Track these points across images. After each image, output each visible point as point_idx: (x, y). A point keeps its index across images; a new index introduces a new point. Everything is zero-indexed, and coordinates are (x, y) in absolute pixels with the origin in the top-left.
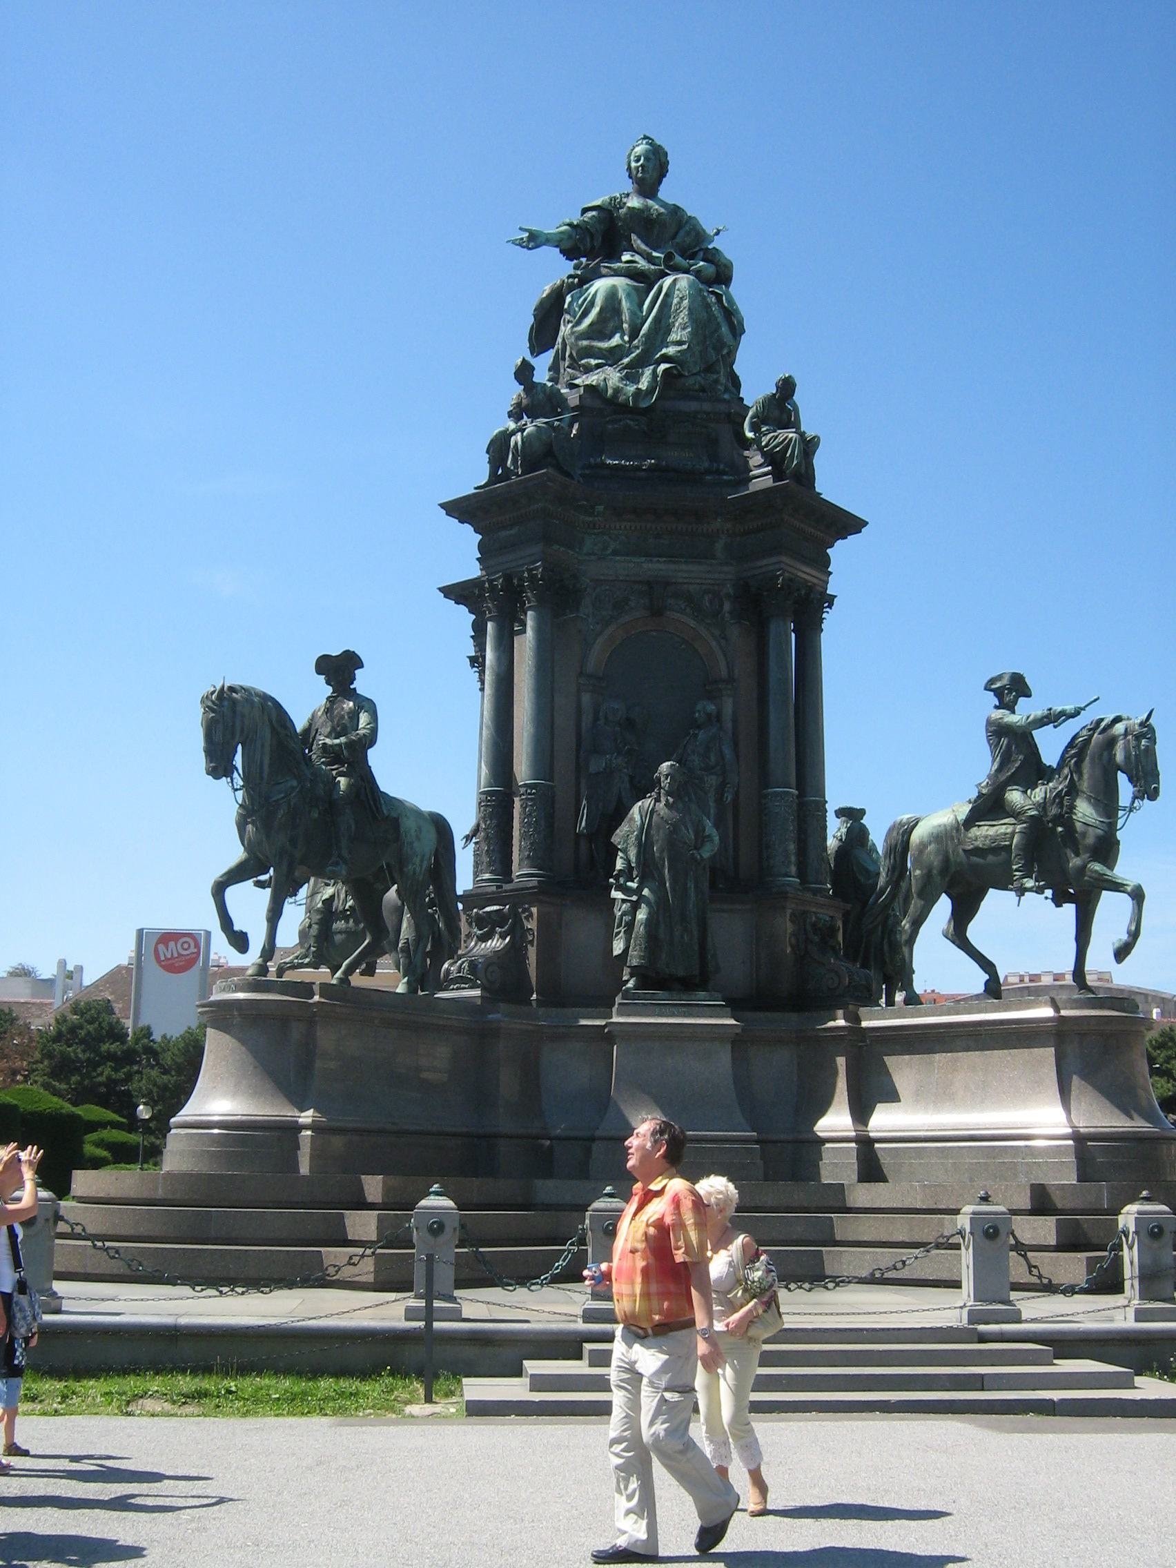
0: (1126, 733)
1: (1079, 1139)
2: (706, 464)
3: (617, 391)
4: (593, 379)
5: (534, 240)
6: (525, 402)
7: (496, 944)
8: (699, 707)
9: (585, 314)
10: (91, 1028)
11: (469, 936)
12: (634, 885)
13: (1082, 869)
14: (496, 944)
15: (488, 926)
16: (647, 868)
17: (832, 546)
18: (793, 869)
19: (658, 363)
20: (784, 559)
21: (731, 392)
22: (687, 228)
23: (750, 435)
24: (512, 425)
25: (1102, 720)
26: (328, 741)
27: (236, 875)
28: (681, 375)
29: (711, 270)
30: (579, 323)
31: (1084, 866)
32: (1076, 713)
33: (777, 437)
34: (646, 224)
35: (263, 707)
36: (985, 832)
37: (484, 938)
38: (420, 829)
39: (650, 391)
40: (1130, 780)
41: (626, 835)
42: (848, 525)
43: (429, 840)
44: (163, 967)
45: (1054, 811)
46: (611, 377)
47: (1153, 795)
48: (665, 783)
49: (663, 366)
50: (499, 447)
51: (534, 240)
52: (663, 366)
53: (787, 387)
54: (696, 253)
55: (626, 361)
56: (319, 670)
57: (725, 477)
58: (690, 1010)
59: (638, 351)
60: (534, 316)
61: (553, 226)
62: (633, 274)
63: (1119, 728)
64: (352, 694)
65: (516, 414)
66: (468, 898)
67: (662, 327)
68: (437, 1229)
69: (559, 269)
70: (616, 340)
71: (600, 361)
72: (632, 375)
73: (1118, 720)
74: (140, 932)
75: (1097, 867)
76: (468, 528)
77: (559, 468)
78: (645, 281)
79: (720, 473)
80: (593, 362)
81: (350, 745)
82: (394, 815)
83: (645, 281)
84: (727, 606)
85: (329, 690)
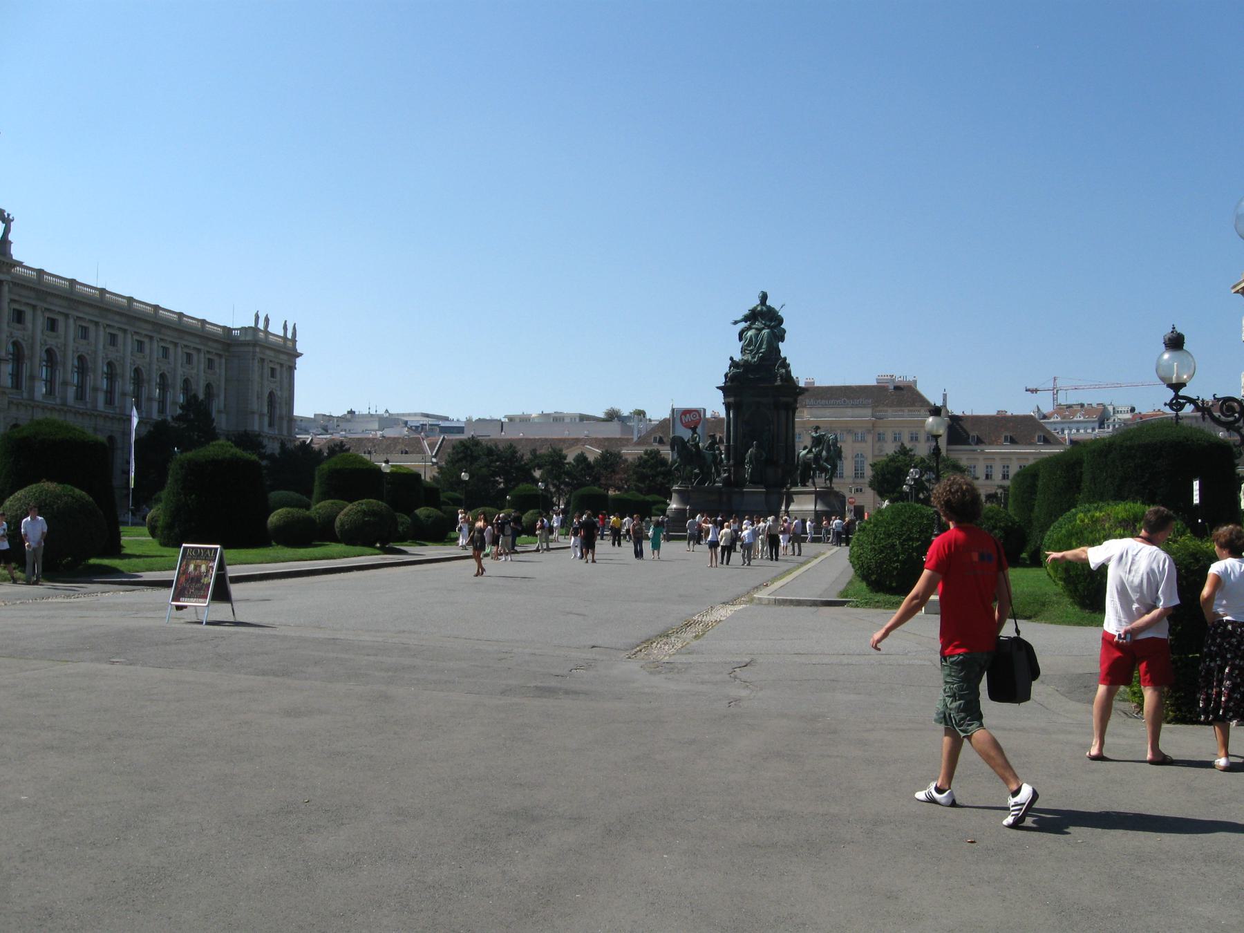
1: (816, 511)
5: (736, 323)
7: (726, 475)
10: (652, 461)
14: (726, 475)
15: (725, 471)
16: (751, 462)
34: (761, 313)
36: (809, 456)
44: (685, 426)
50: (726, 376)
51: (736, 323)
52: (761, 355)
58: (758, 488)
61: (740, 317)
64: (696, 433)
65: (730, 368)
67: (760, 346)
70: (751, 348)
72: (753, 358)
74: (673, 410)
75: (825, 464)
78: (759, 330)
80: (748, 352)
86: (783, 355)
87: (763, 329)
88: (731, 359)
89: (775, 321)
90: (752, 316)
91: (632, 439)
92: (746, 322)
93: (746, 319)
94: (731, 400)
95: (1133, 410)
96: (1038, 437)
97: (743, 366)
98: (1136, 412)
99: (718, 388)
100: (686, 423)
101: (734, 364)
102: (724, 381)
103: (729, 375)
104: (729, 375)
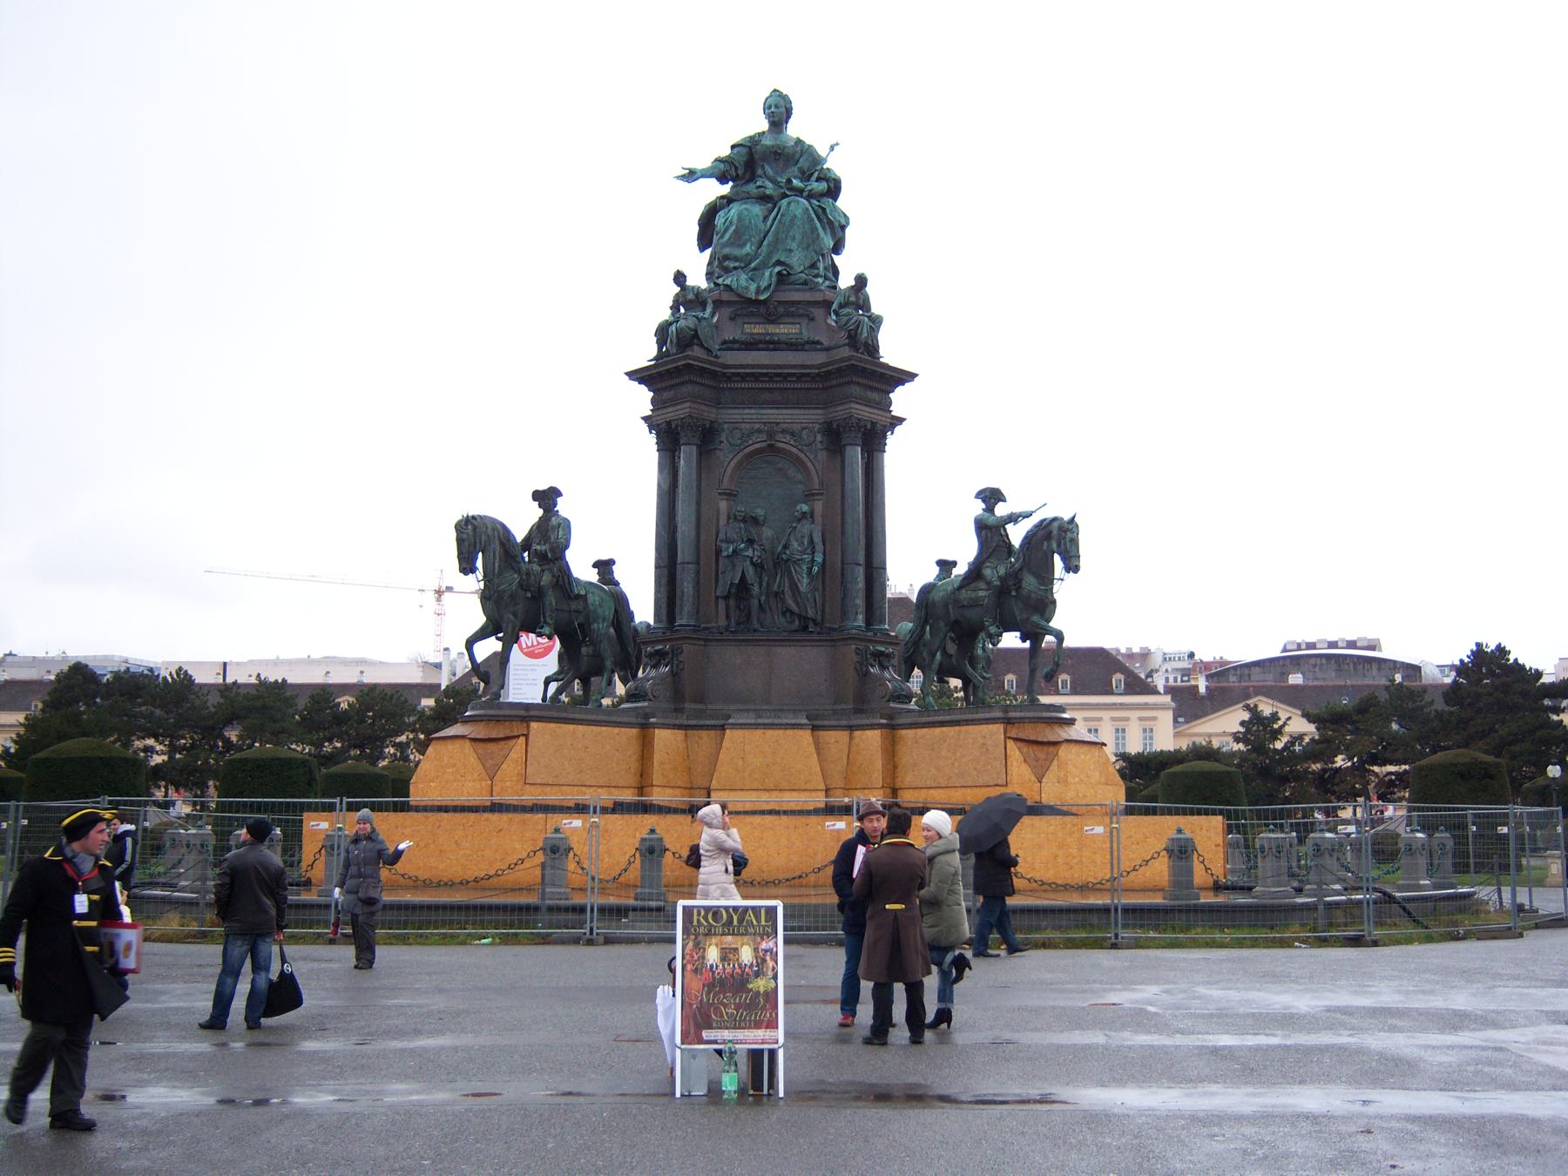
2: (806, 338)
5: (691, 176)
6: (681, 300)
8: (798, 508)
9: (726, 230)
15: (658, 658)
17: (893, 391)
18: (860, 617)
19: (774, 265)
20: (853, 405)
21: (830, 280)
25: (1045, 520)
26: (538, 547)
27: (481, 635)
28: (789, 274)
29: (822, 186)
30: (722, 237)
31: (1028, 619)
32: (1028, 515)
33: (851, 319)
35: (494, 529)
40: (1064, 559)
47: (1076, 569)
49: (778, 269)
50: (662, 332)
51: (691, 176)
52: (778, 269)
53: (861, 281)
54: (813, 174)
55: (753, 265)
56: (534, 499)
57: (819, 347)
60: (699, 225)
61: (704, 162)
62: (764, 199)
63: (1056, 524)
65: (675, 308)
70: (748, 249)
71: (737, 264)
75: (1035, 618)
76: (643, 388)
77: (702, 346)
80: (732, 264)
82: (583, 593)
84: (819, 437)
85: (540, 512)
87: (784, 196)
88: (679, 278)
89: (818, 180)
91: (439, 685)
92: (722, 179)
93: (724, 171)
94: (676, 412)
95: (1191, 655)
98: (1196, 658)
100: (528, 647)
101: (687, 299)
103: (673, 328)
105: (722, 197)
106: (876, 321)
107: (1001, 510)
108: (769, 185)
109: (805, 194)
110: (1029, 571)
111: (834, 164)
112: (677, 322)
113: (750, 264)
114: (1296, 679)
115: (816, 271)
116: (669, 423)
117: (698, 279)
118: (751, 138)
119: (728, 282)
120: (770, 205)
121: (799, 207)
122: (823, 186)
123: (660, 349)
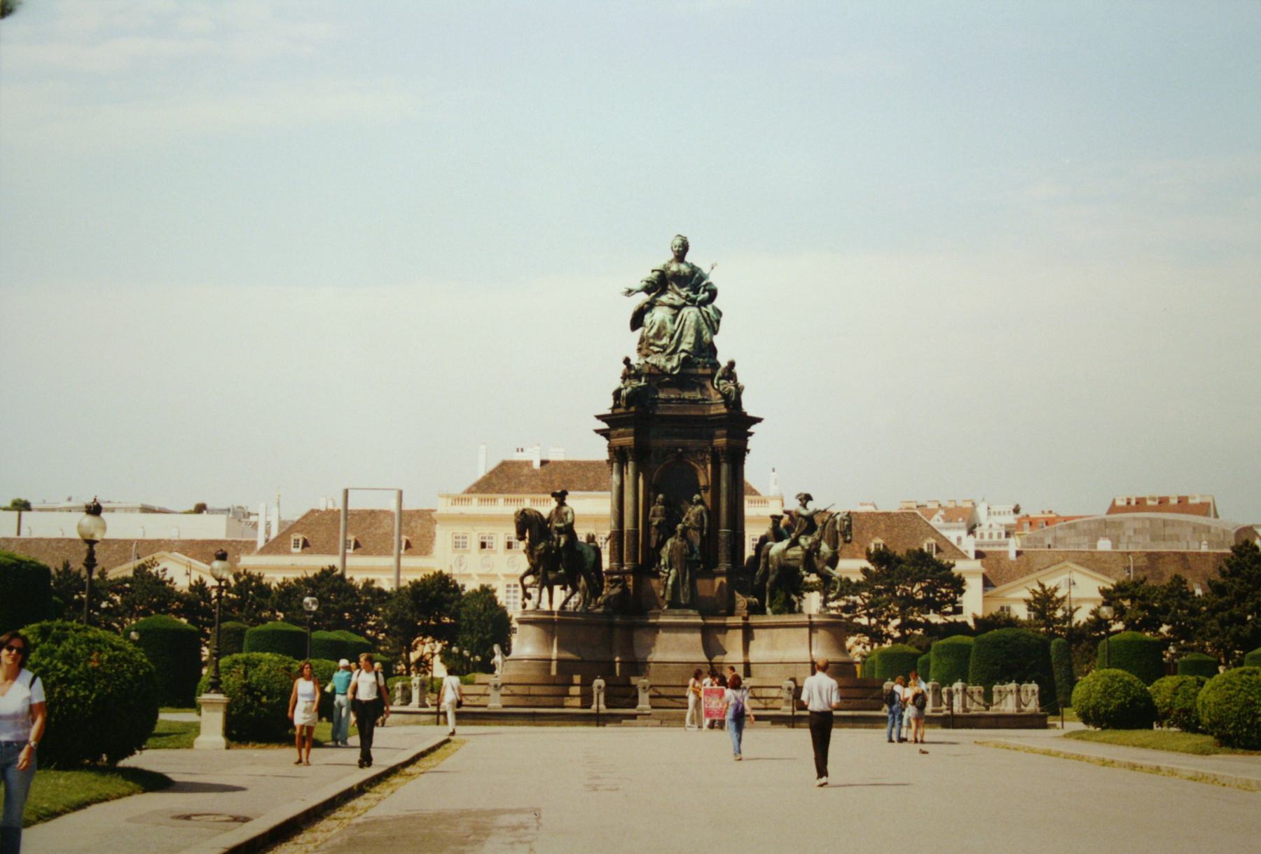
0: (841, 519)
3: (665, 367)
4: (653, 360)
9: (652, 328)
11: (608, 586)
12: (667, 571)
13: (823, 568)
14: (617, 590)
22: (697, 275)
23: (716, 387)
24: (622, 386)
30: (649, 331)
37: (613, 587)
38: (589, 554)
39: (677, 367)
41: (665, 553)
42: (757, 420)
43: (593, 555)
45: (813, 547)
46: (659, 360)
48: (679, 533)
50: (617, 394)
52: (683, 355)
53: (732, 365)
59: (672, 348)
62: (672, 306)
66: (609, 573)
68: (599, 687)
69: (643, 298)
70: (665, 341)
73: (838, 514)
75: (828, 568)
78: (677, 309)
79: (706, 400)
80: (656, 349)
81: (566, 526)
83: (677, 309)
86: (723, 359)
87: (684, 305)
88: (627, 361)
90: (659, 284)
91: (254, 543)
92: (647, 290)
96: (928, 545)
97: (649, 375)
98: (1023, 512)
99: (599, 417)
101: (630, 373)
102: (611, 403)
103: (624, 393)
104: (624, 393)
105: (647, 303)
106: (739, 390)
107: (811, 506)
108: (676, 297)
109: (697, 304)
110: (825, 541)
111: (714, 279)
112: (626, 388)
113: (665, 350)
114: (1104, 545)
115: (704, 355)
116: (621, 447)
117: (636, 360)
118: (665, 265)
119: (654, 362)
120: (676, 311)
121: (690, 314)
122: (707, 294)
123: (615, 403)
